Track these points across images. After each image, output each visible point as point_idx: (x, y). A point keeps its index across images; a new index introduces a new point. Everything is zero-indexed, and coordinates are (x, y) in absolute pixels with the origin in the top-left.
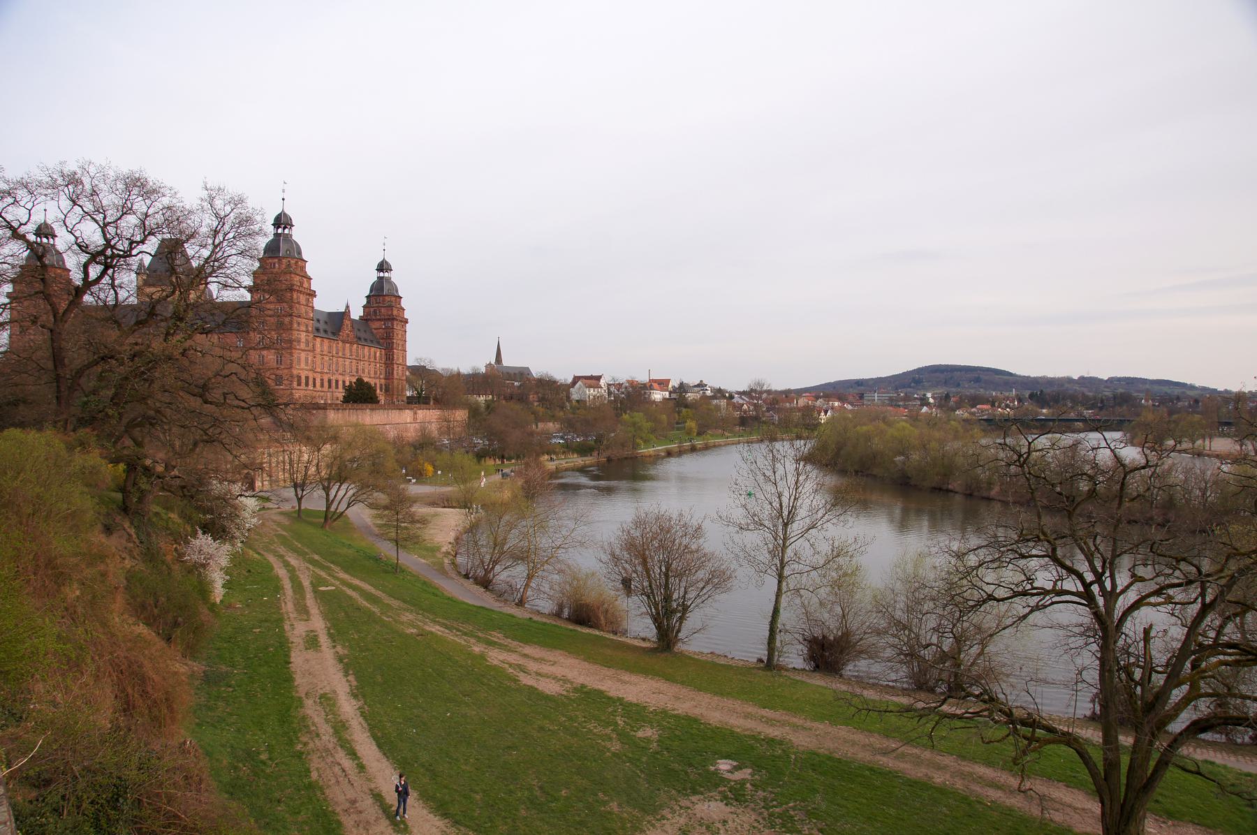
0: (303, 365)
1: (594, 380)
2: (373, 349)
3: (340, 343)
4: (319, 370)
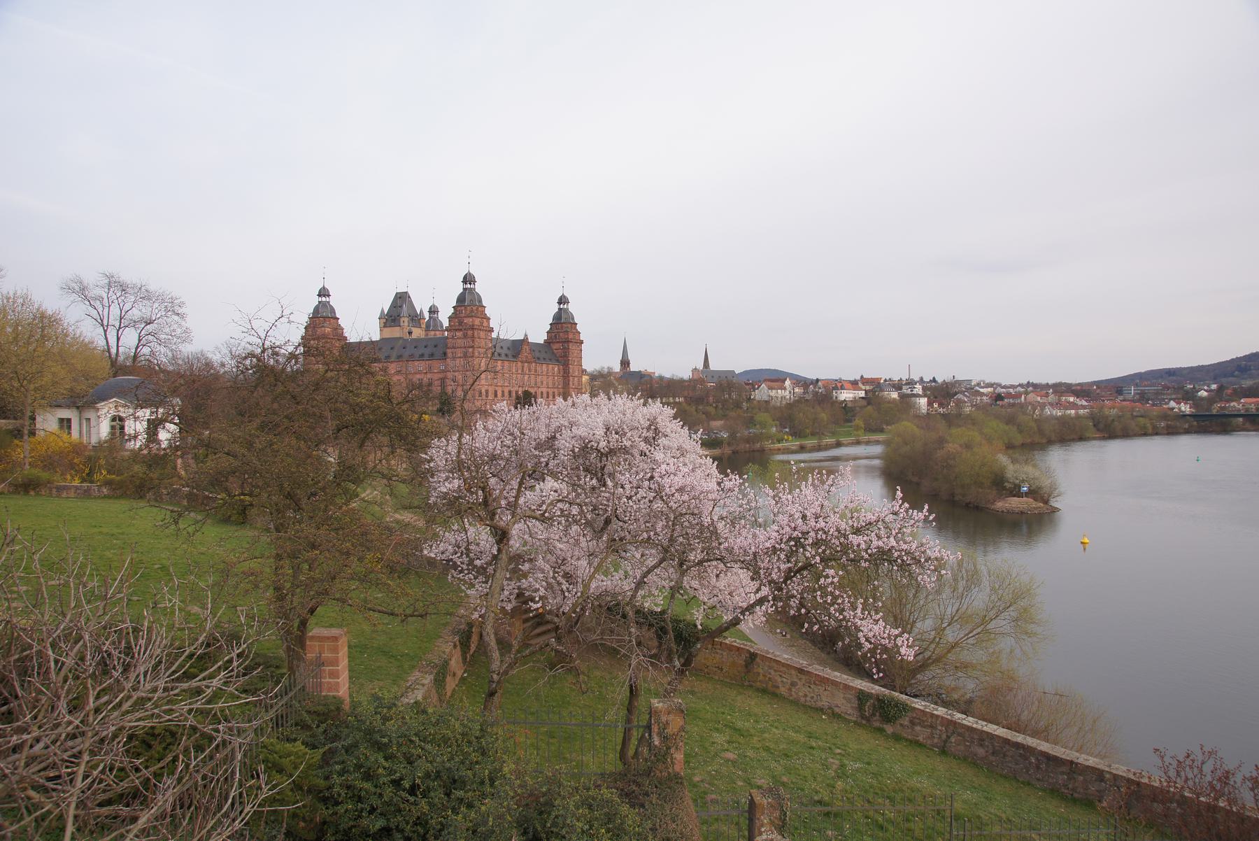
1: (777, 378)
3: (520, 364)
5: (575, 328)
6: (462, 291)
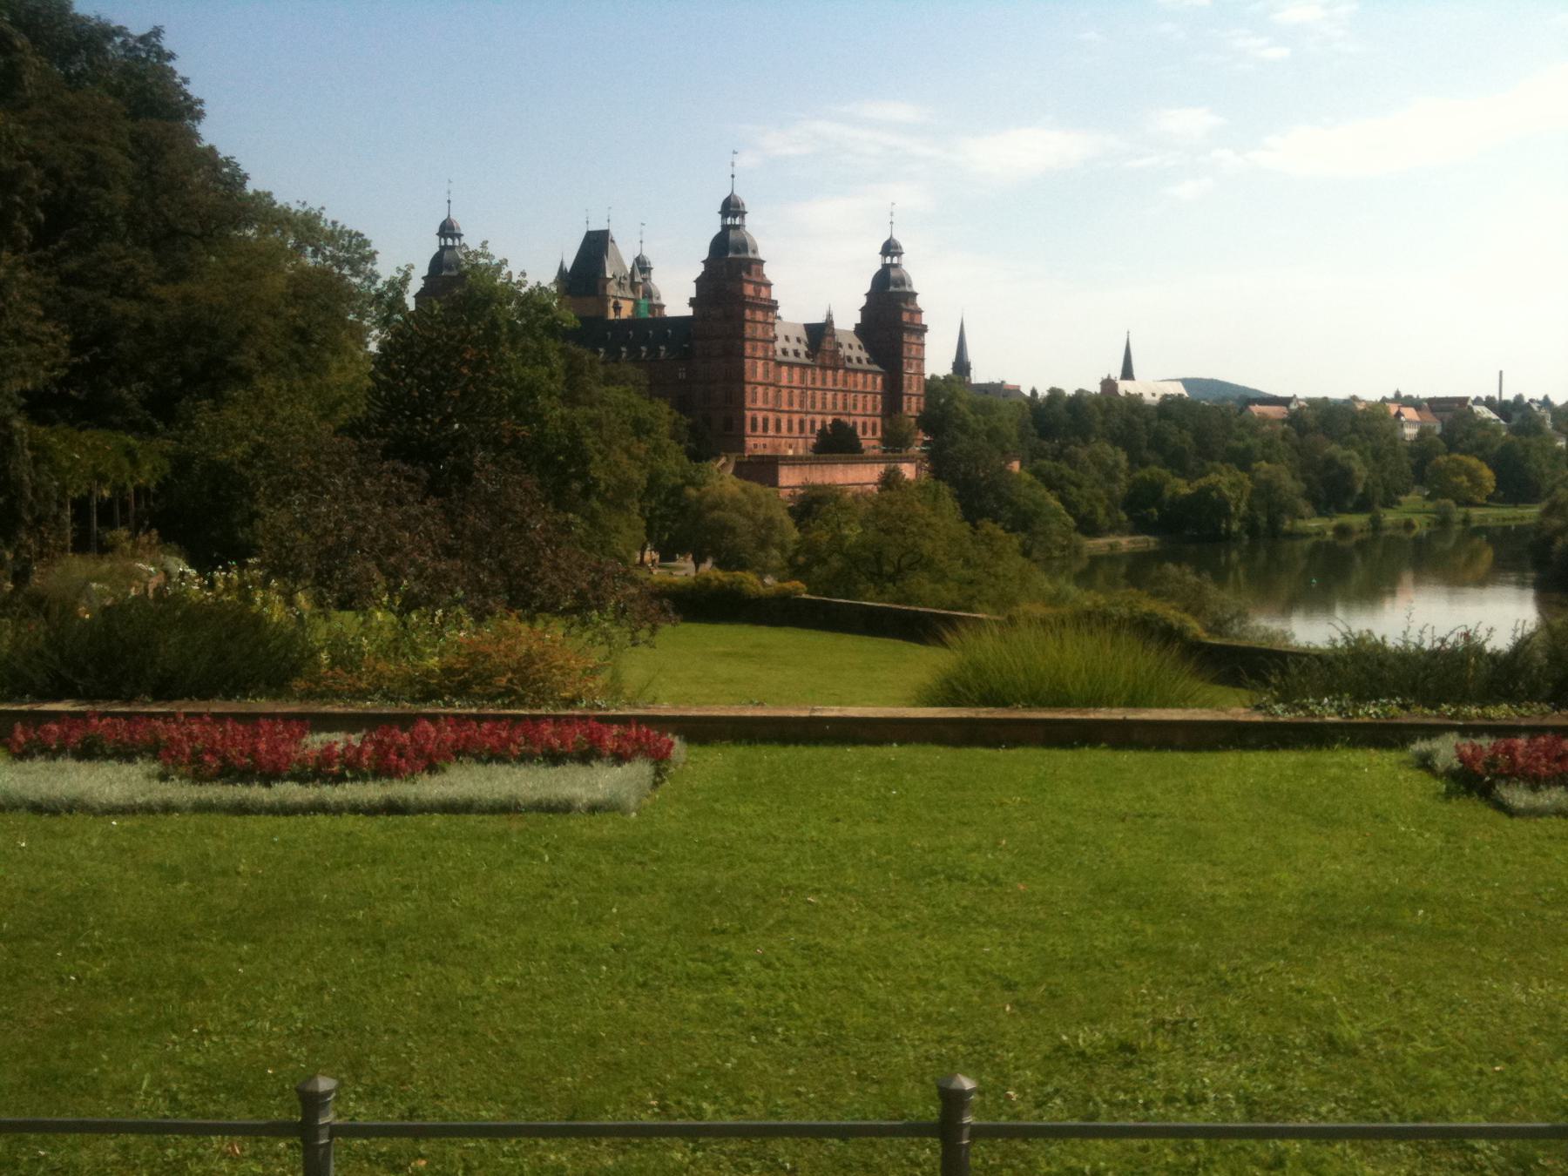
0: (760, 404)
2: (870, 376)
3: (818, 371)
4: (787, 409)
5: (914, 303)
6: (719, 229)
